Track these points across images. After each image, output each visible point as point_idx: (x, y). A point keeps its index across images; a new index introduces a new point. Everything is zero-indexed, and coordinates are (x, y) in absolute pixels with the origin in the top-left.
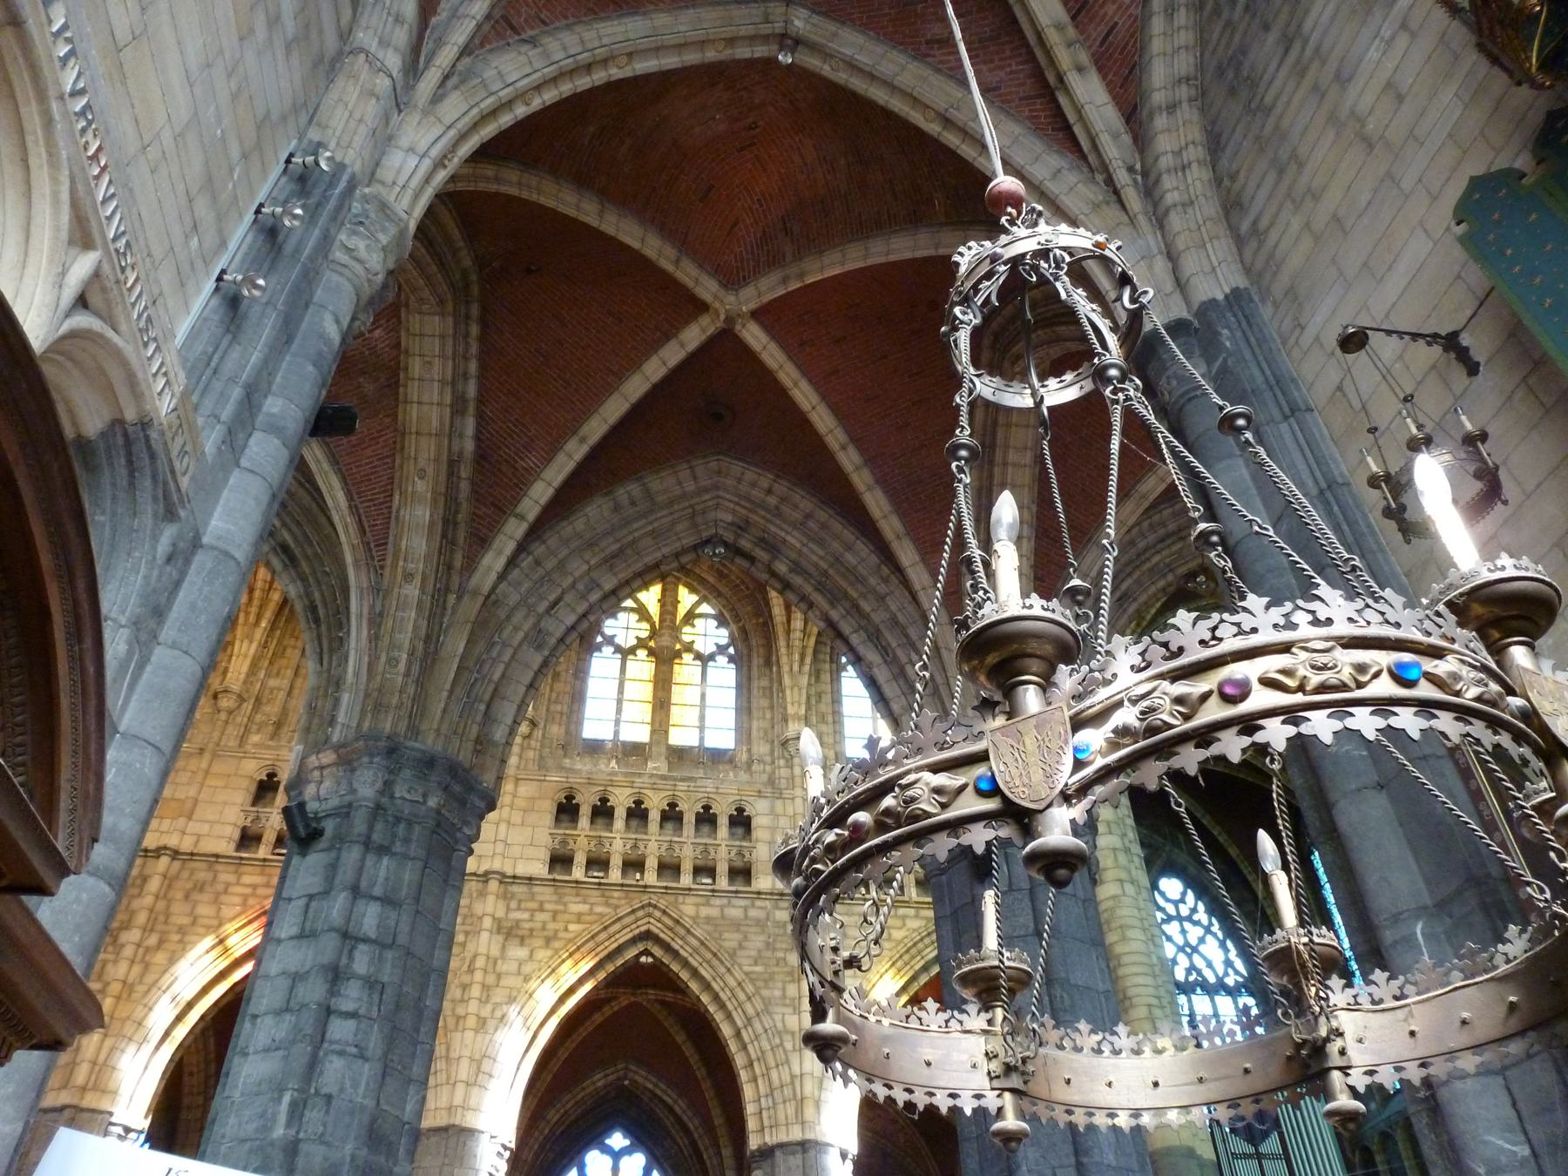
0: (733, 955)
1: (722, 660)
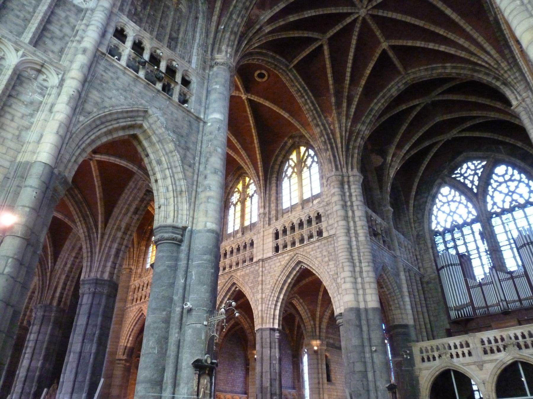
0: (247, 283)
1: (255, 195)
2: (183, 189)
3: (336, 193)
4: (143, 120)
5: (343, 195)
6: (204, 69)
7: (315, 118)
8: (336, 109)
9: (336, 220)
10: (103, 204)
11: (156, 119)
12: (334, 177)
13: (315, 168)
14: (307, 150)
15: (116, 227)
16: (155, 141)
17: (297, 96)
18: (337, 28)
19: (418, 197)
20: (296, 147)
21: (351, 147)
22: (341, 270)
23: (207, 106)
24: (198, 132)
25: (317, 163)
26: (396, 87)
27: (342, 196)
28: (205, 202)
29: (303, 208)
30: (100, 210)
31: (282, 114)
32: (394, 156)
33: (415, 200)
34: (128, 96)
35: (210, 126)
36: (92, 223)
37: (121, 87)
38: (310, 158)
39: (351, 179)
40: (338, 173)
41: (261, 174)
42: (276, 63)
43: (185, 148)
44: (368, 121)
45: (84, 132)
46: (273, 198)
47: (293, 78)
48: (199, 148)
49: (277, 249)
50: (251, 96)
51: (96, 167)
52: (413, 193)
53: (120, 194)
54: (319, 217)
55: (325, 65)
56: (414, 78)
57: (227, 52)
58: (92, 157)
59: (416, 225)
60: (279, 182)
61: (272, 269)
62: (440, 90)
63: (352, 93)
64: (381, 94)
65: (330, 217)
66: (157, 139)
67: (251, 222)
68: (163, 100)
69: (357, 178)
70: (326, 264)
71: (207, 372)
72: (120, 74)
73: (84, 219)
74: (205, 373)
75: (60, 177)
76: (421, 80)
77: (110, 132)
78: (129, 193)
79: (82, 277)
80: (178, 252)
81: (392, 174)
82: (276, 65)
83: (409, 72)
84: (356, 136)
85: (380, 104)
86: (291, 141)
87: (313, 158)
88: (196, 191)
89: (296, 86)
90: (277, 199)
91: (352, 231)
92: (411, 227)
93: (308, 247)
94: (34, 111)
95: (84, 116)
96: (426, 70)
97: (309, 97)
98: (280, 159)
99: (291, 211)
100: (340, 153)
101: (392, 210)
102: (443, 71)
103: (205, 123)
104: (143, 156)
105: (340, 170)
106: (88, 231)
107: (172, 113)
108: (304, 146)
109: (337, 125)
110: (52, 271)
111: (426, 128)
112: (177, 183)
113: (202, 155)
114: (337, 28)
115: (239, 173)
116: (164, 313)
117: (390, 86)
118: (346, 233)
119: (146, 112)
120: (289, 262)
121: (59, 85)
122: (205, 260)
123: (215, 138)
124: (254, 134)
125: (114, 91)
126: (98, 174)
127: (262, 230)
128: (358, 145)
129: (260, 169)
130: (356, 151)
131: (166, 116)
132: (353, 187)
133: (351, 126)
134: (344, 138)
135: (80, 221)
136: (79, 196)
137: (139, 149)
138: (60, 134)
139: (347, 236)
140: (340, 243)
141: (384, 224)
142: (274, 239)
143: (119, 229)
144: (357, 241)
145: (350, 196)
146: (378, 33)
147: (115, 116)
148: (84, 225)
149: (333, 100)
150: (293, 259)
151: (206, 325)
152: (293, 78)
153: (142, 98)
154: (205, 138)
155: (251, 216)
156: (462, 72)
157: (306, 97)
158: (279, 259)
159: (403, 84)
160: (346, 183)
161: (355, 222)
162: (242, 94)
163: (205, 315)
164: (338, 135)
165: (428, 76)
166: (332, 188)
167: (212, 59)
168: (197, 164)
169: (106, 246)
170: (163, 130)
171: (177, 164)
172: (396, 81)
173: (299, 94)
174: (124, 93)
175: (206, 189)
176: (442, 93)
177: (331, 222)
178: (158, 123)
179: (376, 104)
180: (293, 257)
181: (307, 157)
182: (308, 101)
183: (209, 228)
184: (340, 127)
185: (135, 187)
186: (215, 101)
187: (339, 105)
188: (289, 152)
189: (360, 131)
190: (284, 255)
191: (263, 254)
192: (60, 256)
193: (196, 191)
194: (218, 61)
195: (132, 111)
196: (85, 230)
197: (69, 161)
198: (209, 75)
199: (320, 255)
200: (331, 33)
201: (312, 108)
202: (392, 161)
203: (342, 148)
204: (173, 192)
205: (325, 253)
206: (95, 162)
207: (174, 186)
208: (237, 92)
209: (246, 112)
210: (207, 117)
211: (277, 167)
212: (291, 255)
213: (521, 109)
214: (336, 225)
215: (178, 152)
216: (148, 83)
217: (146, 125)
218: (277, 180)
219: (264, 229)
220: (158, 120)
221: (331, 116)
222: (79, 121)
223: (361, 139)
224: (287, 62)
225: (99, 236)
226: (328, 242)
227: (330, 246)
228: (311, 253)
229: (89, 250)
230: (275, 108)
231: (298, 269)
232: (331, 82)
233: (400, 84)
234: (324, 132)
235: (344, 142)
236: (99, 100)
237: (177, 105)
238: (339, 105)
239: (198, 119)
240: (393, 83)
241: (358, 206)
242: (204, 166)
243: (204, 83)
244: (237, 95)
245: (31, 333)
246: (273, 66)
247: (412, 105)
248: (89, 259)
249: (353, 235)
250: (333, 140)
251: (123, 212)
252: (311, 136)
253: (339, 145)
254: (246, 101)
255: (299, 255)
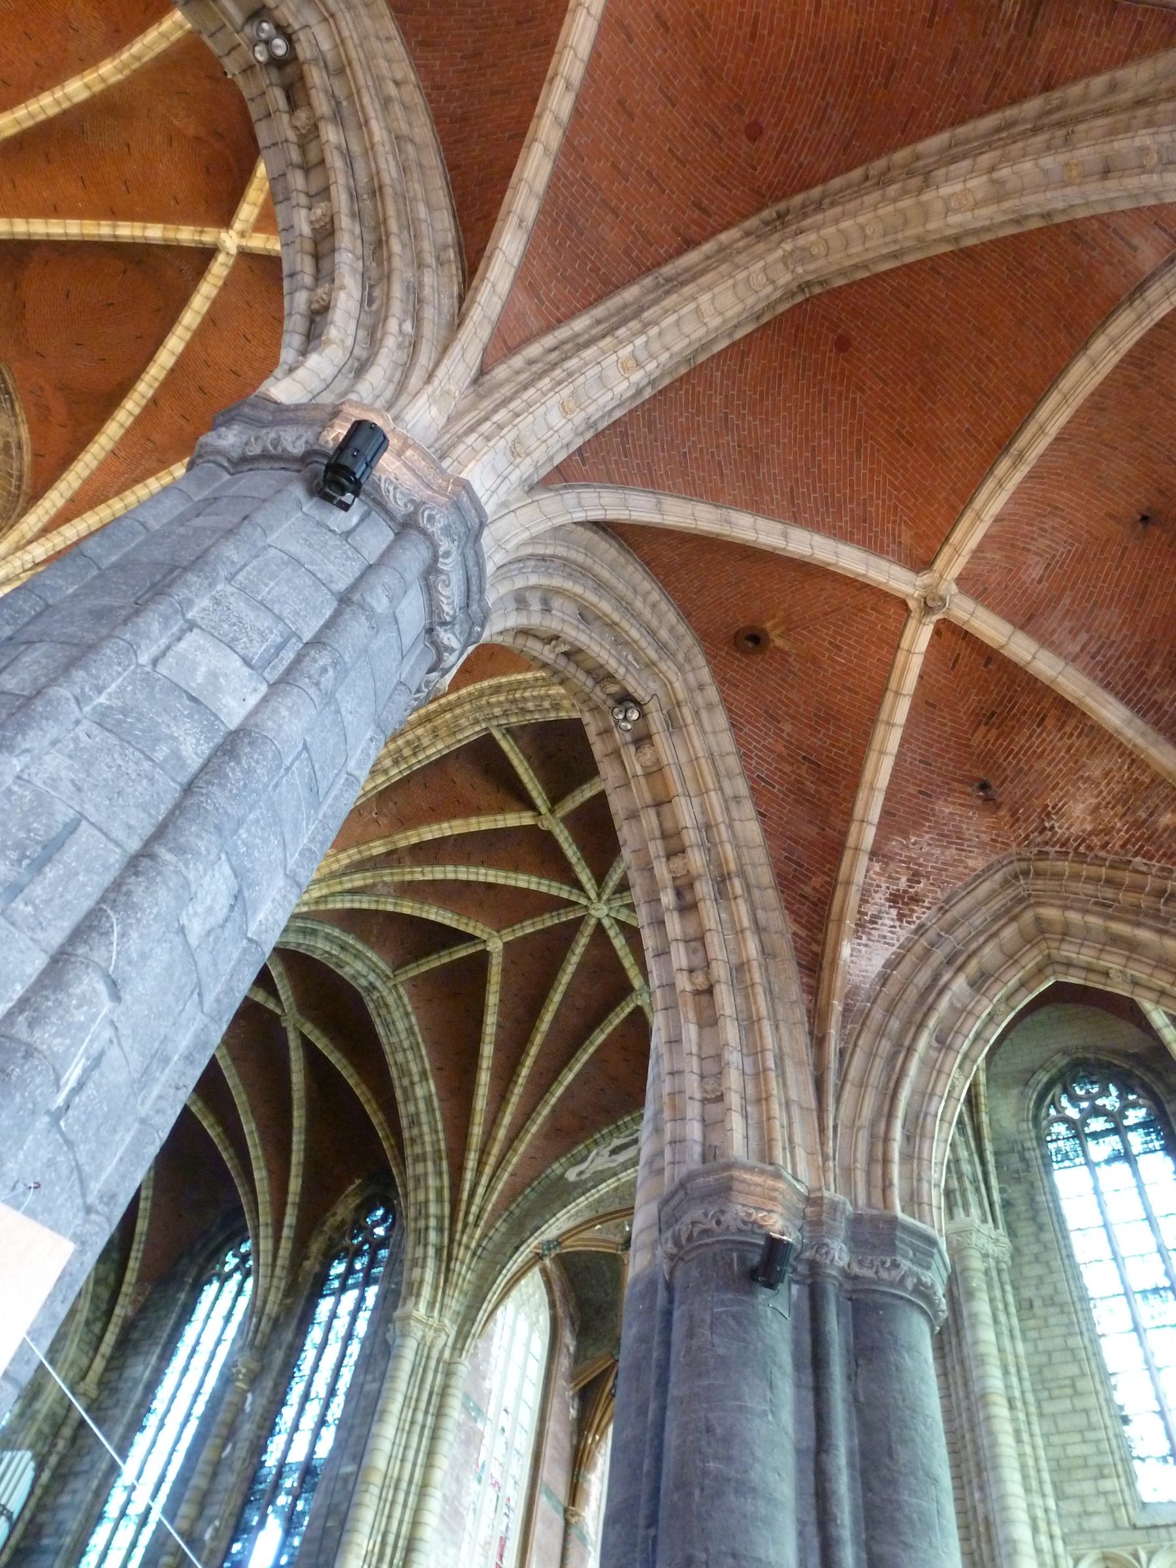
18: (571, 852)
56: (387, 1006)
62: (322, 1043)
64: (351, 940)
83: (401, 990)
89: (433, 744)
96: (410, 1031)
102: (416, 1078)
114: (571, 852)
146: (528, 928)
156: (426, 1128)
165: (394, 1040)
176: (307, 1045)
200: (563, 836)
213: (419, 1334)
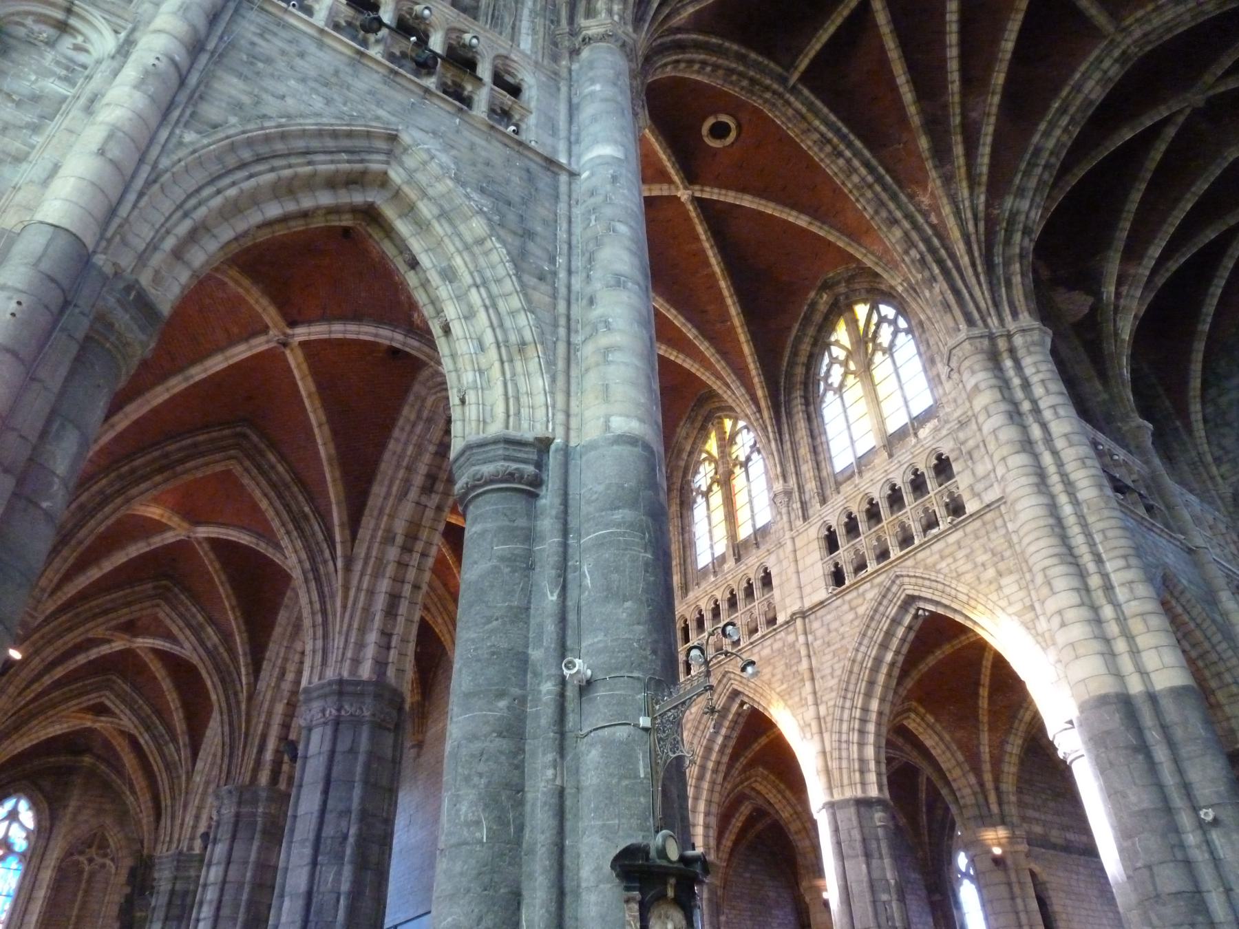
0: (769, 684)
1: (755, 456)
2: (528, 336)
3: (983, 386)
4: (388, 163)
5: (1004, 386)
6: (555, 58)
7: (883, 204)
8: (936, 167)
9: (996, 458)
10: (337, 474)
11: (425, 157)
12: (967, 345)
13: (906, 347)
14: (874, 307)
15: (380, 533)
16: (429, 216)
17: (819, 156)
19: (1213, 392)
20: (842, 308)
21: (998, 260)
22: (1045, 591)
23: (573, 138)
24: (557, 198)
25: (909, 331)
26: (1097, 75)
27: (1000, 388)
28: (598, 365)
29: (891, 456)
30: (334, 492)
31: (791, 219)
32: (1119, 283)
33: (1204, 403)
34: (336, 96)
35: (589, 178)
36: (320, 536)
37: (313, 73)
38: (885, 326)
39: (1018, 340)
40: (976, 332)
41: (760, 393)
42: (751, 73)
43: (520, 232)
44: (1033, 183)
45: (200, 176)
46: (804, 451)
47: (804, 110)
48: (562, 235)
49: (838, 577)
50: (702, 191)
51: (305, 366)
52: (1196, 383)
53: (381, 446)
54: (943, 467)
55: (882, 50)
56: (1146, 35)
57: (610, 12)
58: (285, 334)
59: (1224, 468)
60: (812, 408)
61: (833, 634)
63: (974, 115)
65: (976, 455)
66: (436, 211)
67: (754, 526)
68: (443, 114)
69: (1036, 336)
70: (993, 587)
71: (671, 893)
72: (312, 48)
73: (298, 528)
74: (662, 897)
75: (121, 285)
76: (1169, 36)
77: (288, 189)
78: (403, 437)
79: (304, 683)
80: (532, 514)
81: (1126, 329)
82: (753, 81)
83: (1127, 22)
84: (1006, 231)
85: (1058, 132)
86: (825, 296)
87: (894, 322)
88: (569, 343)
89: (816, 130)
90: (815, 451)
91: (1054, 479)
92: (1212, 478)
93: (927, 552)
94: (42, 117)
95: (199, 132)
97: (857, 154)
98: (805, 347)
99: (860, 472)
100: (972, 280)
101: (1151, 426)
103: (573, 175)
104: (402, 267)
105: (980, 323)
106: (312, 559)
107: (472, 147)
108: (865, 301)
109: (947, 210)
110: (250, 698)
111: (1202, 186)
112: (508, 323)
113: (575, 251)
115: (704, 411)
116: (502, 704)
117: (1077, 76)
118: (1037, 485)
119: (393, 138)
120: (880, 603)
121: (118, 52)
122: (619, 525)
123: (607, 200)
124: (726, 293)
125: (292, 83)
126: (313, 389)
127: (788, 535)
128: (1017, 250)
129: (756, 380)
130: (1017, 267)
131: (454, 152)
132: (1027, 361)
133: (988, 205)
134: (973, 238)
135: (288, 533)
136: (280, 468)
137: (389, 249)
138: (109, 155)
139: (1040, 492)
140: (1023, 517)
141: (1137, 464)
142: (825, 552)
143: (389, 539)
144: (1075, 502)
145: (1026, 385)
147: (300, 144)
148: (299, 544)
149: (924, 143)
150: (890, 596)
151: (646, 730)
152: (804, 110)
153: (379, 104)
154: (577, 211)
155: (752, 511)
157: (848, 153)
158: (850, 602)
159: (1116, 61)
160: (1005, 355)
161: (1055, 453)
162: (677, 188)
163: (641, 696)
164: (955, 234)
165: (1187, 17)
166: (966, 376)
167: (573, 34)
168: (562, 275)
169: (359, 589)
170: (450, 184)
171: (501, 271)
172: (1092, 58)
173: (828, 149)
174: (323, 90)
175: (595, 330)
177: (981, 470)
178: (434, 167)
179: (1047, 134)
180: (889, 589)
181: (878, 325)
182: (856, 163)
183: (619, 432)
184: (957, 213)
185: (419, 417)
186: (594, 119)
187: (941, 153)
188: (827, 326)
189: (1013, 215)
190: (861, 589)
191: (802, 598)
192: (268, 655)
193: (569, 343)
194: (590, 32)
195: (350, 135)
196: (304, 556)
197: (153, 246)
198: (570, 71)
199: (969, 566)
201: (870, 179)
202: (1118, 295)
203: (973, 265)
204: (499, 347)
205: (982, 558)
206: (299, 353)
207: (498, 331)
208: (665, 186)
209: (697, 238)
210: (578, 162)
211: (800, 371)
212: (880, 585)
214: (1000, 471)
215: (504, 243)
216: (392, 71)
217: (396, 175)
218: (807, 404)
219: (794, 533)
220: (433, 158)
221: (925, 189)
222: (180, 144)
223: (1024, 233)
224: (779, 69)
225: (340, 564)
226: (984, 524)
227: (993, 536)
228: (938, 567)
229: (317, 606)
230: (769, 208)
231: (907, 619)
232: (908, 95)
233: (1106, 64)
234: (914, 236)
235: (975, 247)
236: (246, 100)
237: (484, 128)
238: (941, 153)
239: (550, 163)
240: (1083, 68)
241: (1053, 407)
242: (584, 275)
243: (559, 89)
244: (665, 193)
245: (209, 865)
246: (745, 83)
247: (1149, 123)
248: (320, 632)
249: (1058, 488)
250: (943, 252)
251: (395, 489)
252: (880, 258)
253: (965, 261)
254: (691, 208)
255: (906, 580)
